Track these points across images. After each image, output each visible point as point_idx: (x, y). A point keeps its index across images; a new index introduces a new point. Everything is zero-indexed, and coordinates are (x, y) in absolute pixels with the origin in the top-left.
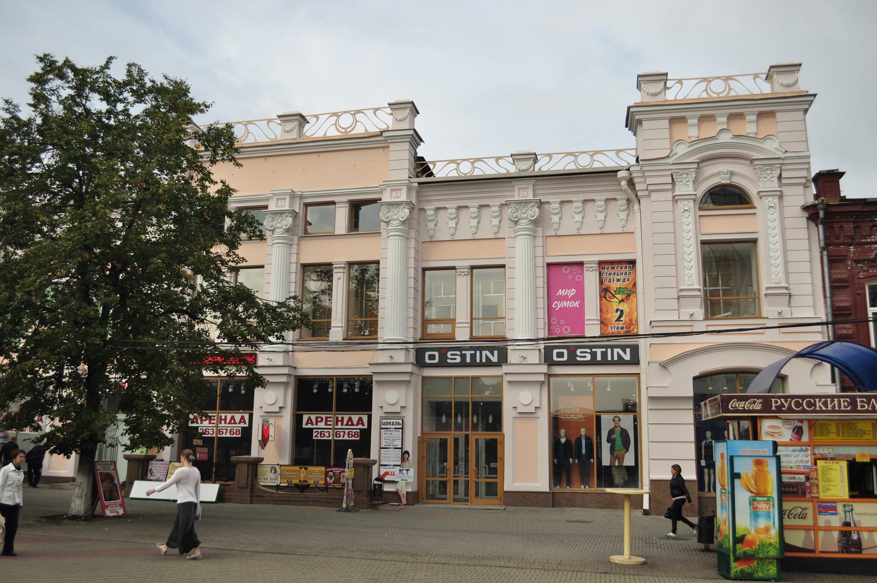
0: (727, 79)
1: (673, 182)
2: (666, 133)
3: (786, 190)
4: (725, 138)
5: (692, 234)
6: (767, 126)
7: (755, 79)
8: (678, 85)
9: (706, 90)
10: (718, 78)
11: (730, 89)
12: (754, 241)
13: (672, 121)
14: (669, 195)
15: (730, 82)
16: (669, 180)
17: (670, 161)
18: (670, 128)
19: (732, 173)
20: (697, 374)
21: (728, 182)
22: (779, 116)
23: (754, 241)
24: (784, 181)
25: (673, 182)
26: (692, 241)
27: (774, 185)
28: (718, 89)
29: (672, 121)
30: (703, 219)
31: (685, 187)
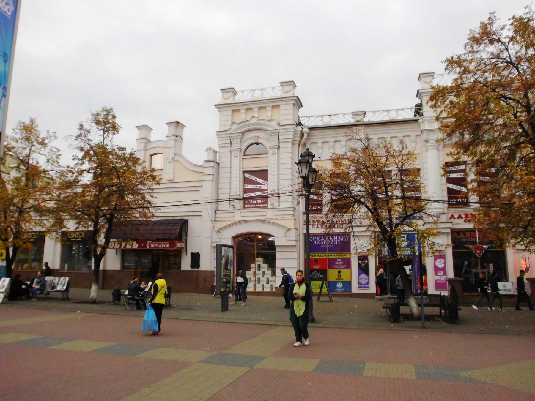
0: (262, 90)
1: (231, 142)
2: (230, 118)
3: (281, 145)
4: (254, 121)
5: (238, 168)
6: (276, 112)
7: (272, 90)
8: (242, 93)
9: (252, 96)
10: (258, 89)
11: (263, 95)
12: (267, 170)
13: (233, 111)
14: (229, 149)
15: (263, 91)
16: (229, 142)
17: (229, 132)
18: (232, 116)
19: (258, 137)
20: (233, 235)
21: (256, 142)
22: (282, 107)
23: (267, 170)
24: (280, 141)
25: (231, 142)
26: (238, 172)
27: (276, 143)
28: (258, 95)
29: (233, 111)
30: (244, 160)
31: (236, 145)
